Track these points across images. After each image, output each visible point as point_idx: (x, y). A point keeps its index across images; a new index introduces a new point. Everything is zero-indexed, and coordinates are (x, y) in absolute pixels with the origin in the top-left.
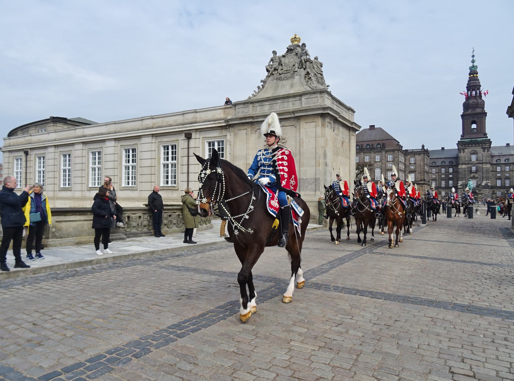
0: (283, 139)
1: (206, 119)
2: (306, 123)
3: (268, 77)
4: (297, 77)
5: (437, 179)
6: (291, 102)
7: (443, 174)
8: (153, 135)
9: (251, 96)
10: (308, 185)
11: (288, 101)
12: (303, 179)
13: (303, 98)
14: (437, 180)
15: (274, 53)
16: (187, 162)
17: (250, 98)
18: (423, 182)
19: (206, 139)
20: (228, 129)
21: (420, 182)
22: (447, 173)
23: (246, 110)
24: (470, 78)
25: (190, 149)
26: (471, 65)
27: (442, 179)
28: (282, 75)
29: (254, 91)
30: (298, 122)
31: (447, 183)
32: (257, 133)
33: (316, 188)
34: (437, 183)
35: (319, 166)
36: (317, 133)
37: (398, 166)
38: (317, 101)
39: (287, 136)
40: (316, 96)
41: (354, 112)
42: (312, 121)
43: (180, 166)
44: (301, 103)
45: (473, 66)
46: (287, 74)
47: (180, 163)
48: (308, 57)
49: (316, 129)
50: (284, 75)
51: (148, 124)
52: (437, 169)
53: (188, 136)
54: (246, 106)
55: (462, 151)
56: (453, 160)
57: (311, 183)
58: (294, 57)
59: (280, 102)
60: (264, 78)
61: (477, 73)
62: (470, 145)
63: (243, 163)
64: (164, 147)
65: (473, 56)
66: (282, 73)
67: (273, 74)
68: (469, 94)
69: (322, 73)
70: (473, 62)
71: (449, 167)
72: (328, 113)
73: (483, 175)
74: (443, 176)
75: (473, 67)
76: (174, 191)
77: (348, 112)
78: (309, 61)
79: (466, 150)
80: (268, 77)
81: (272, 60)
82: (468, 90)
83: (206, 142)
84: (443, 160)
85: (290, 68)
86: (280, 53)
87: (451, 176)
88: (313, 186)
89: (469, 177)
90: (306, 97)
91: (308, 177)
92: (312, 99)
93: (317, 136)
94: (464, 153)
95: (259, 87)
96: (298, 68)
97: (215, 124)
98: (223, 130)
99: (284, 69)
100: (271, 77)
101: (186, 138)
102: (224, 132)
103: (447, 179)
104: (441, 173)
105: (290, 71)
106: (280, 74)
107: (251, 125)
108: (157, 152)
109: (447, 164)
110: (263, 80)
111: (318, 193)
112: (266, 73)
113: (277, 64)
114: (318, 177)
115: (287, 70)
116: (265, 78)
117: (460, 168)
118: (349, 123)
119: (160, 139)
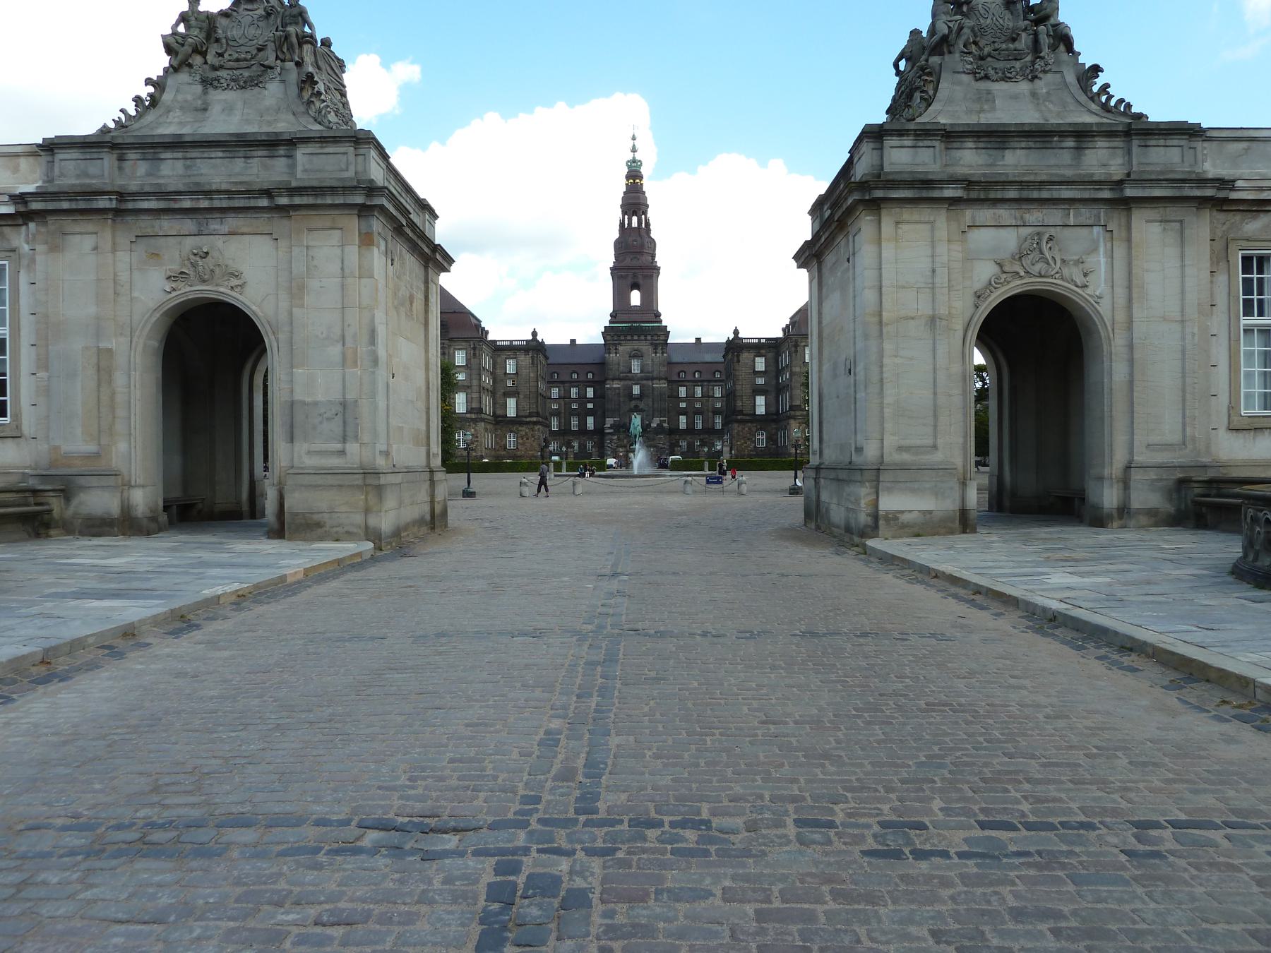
0: (232, 274)
2: (310, 230)
3: (171, 69)
6: (256, 160)
7: (575, 401)
9: (112, 125)
10: (321, 423)
12: (304, 403)
13: (301, 153)
14: (563, 415)
17: (105, 130)
18: (535, 419)
20: (24, 228)
21: (528, 419)
22: (582, 398)
26: (630, 156)
27: (573, 413)
29: (122, 111)
31: (583, 423)
33: (345, 431)
34: (563, 421)
35: (356, 366)
36: (346, 263)
37: (480, 379)
38: (344, 167)
40: (342, 150)
41: (436, 217)
44: (293, 167)
45: (634, 161)
46: (241, 71)
48: (307, 29)
49: (342, 251)
52: (562, 388)
54: (95, 156)
57: (328, 415)
58: (260, 24)
59: (220, 154)
60: (156, 72)
61: (641, 178)
62: (629, 337)
67: (190, 66)
69: (342, 88)
70: (634, 150)
72: (382, 208)
74: (575, 406)
77: (421, 214)
79: (621, 348)
80: (172, 70)
81: (183, 18)
82: (624, 213)
84: (573, 368)
85: (249, 56)
87: (590, 406)
88: (335, 427)
91: (320, 398)
92: (329, 156)
93: (347, 271)
94: (616, 353)
95: (138, 100)
99: (226, 56)
100: (183, 77)
106: (214, 68)
107: (113, 220)
110: (155, 79)
111: (352, 448)
112: (165, 60)
114: (350, 396)
115: (238, 60)
116: (161, 74)
118: (428, 247)
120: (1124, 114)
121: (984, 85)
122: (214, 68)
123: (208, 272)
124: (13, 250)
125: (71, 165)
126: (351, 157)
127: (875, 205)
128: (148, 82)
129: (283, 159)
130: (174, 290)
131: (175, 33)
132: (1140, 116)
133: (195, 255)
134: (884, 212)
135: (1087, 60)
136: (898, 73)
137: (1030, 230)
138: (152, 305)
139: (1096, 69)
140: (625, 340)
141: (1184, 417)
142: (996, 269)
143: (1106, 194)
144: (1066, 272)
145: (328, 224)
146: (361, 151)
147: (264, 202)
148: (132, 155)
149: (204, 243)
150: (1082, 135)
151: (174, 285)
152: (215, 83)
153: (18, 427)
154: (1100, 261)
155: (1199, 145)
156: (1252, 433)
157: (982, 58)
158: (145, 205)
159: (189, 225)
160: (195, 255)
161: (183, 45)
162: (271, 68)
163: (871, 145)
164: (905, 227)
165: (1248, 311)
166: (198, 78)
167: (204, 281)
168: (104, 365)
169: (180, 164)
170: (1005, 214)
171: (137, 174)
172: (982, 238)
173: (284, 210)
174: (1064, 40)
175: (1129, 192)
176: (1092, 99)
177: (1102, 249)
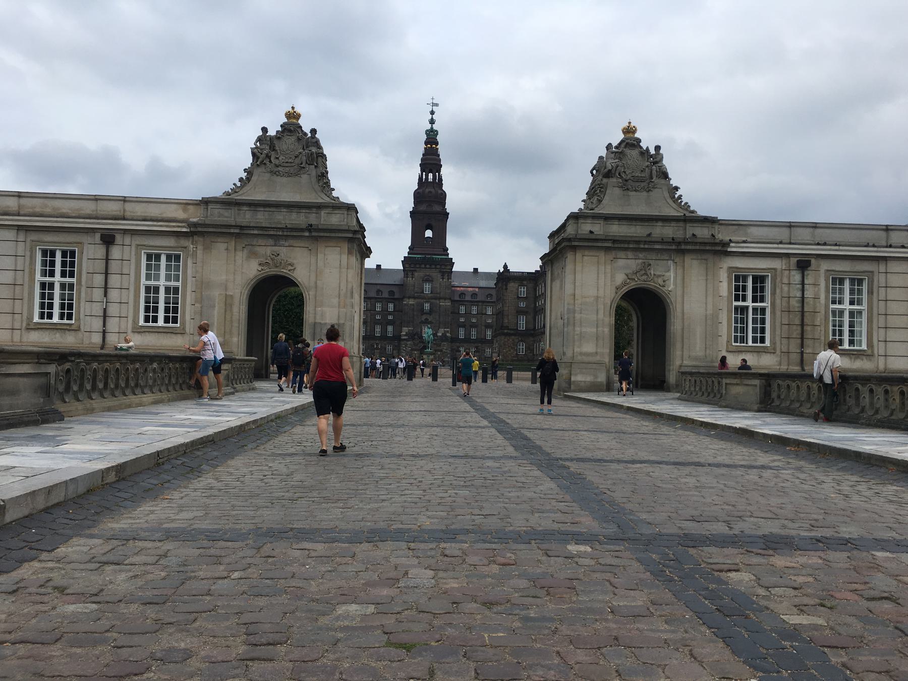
1: (146, 215)
2: (326, 246)
4: (305, 177)
5: (369, 320)
7: (379, 313)
8: (19, 228)
11: (299, 211)
13: (323, 213)
14: (369, 324)
15: (264, 130)
16: (104, 283)
19: (144, 247)
22: (385, 311)
23: (226, 213)
24: (425, 148)
25: (110, 261)
26: (429, 127)
27: (377, 322)
28: (280, 169)
29: (234, 184)
30: (313, 243)
31: (384, 330)
32: (245, 249)
34: (368, 328)
39: (295, 262)
42: (335, 245)
43: (83, 289)
45: (432, 130)
47: (83, 283)
50: (283, 168)
51: (8, 207)
52: (369, 303)
53: (108, 239)
55: (410, 274)
56: (395, 289)
61: (437, 144)
62: (423, 266)
63: (220, 294)
64: (44, 253)
65: (432, 113)
67: (265, 164)
68: (424, 177)
70: (432, 122)
71: (389, 300)
73: (439, 318)
74: (378, 317)
75: (432, 132)
76: (67, 332)
78: (321, 156)
79: (416, 274)
81: (259, 139)
82: (422, 171)
83: (143, 253)
84: (378, 287)
86: (272, 132)
87: (390, 317)
89: (420, 321)
90: (327, 212)
91: (328, 321)
94: (412, 278)
96: (307, 163)
97: (167, 226)
98: (180, 237)
100: (260, 170)
101: (101, 242)
102: (184, 242)
103: (385, 323)
104: (375, 310)
106: (277, 166)
108: (28, 259)
109: (386, 295)
113: (268, 147)
117: (405, 304)
119: (34, 236)
120: (686, 210)
121: (625, 193)
122: (277, 166)
123: (278, 262)
124: (186, 248)
125: (216, 211)
126: (346, 216)
127: (574, 248)
128: (245, 170)
130: (262, 270)
131: (257, 147)
132: (693, 212)
133: (273, 255)
135: (674, 183)
136: (593, 175)
137: (641, 261)
138: (252, 276)
139: (677, 188)
140: (420, 268)
141: (706, 345)
142: (626, 277)
143: (674, 247)
144: (656, 279)
145: (335, 245)
146: (350, 213)
147: (307, 234)
148: (245, 208)
150: (666, 220)
151: (262, 268)
153: (184, 329)
155: (717, 226)
156: (737, 354)
157: (626, 181)
158: (252, 232)
159: (271, 242)
160: (273, 255)
161: (261, 154)
162: (304, 168)
163: (574, 221)
164: (586, 258)
167: (277, 267)
168: (228, 302)
169: (266, 213)
171: (246, 217)
172: (621, 263)
173: (316, 239)
175: (683, 247)
176: (674, 202)
177: (672, 271)
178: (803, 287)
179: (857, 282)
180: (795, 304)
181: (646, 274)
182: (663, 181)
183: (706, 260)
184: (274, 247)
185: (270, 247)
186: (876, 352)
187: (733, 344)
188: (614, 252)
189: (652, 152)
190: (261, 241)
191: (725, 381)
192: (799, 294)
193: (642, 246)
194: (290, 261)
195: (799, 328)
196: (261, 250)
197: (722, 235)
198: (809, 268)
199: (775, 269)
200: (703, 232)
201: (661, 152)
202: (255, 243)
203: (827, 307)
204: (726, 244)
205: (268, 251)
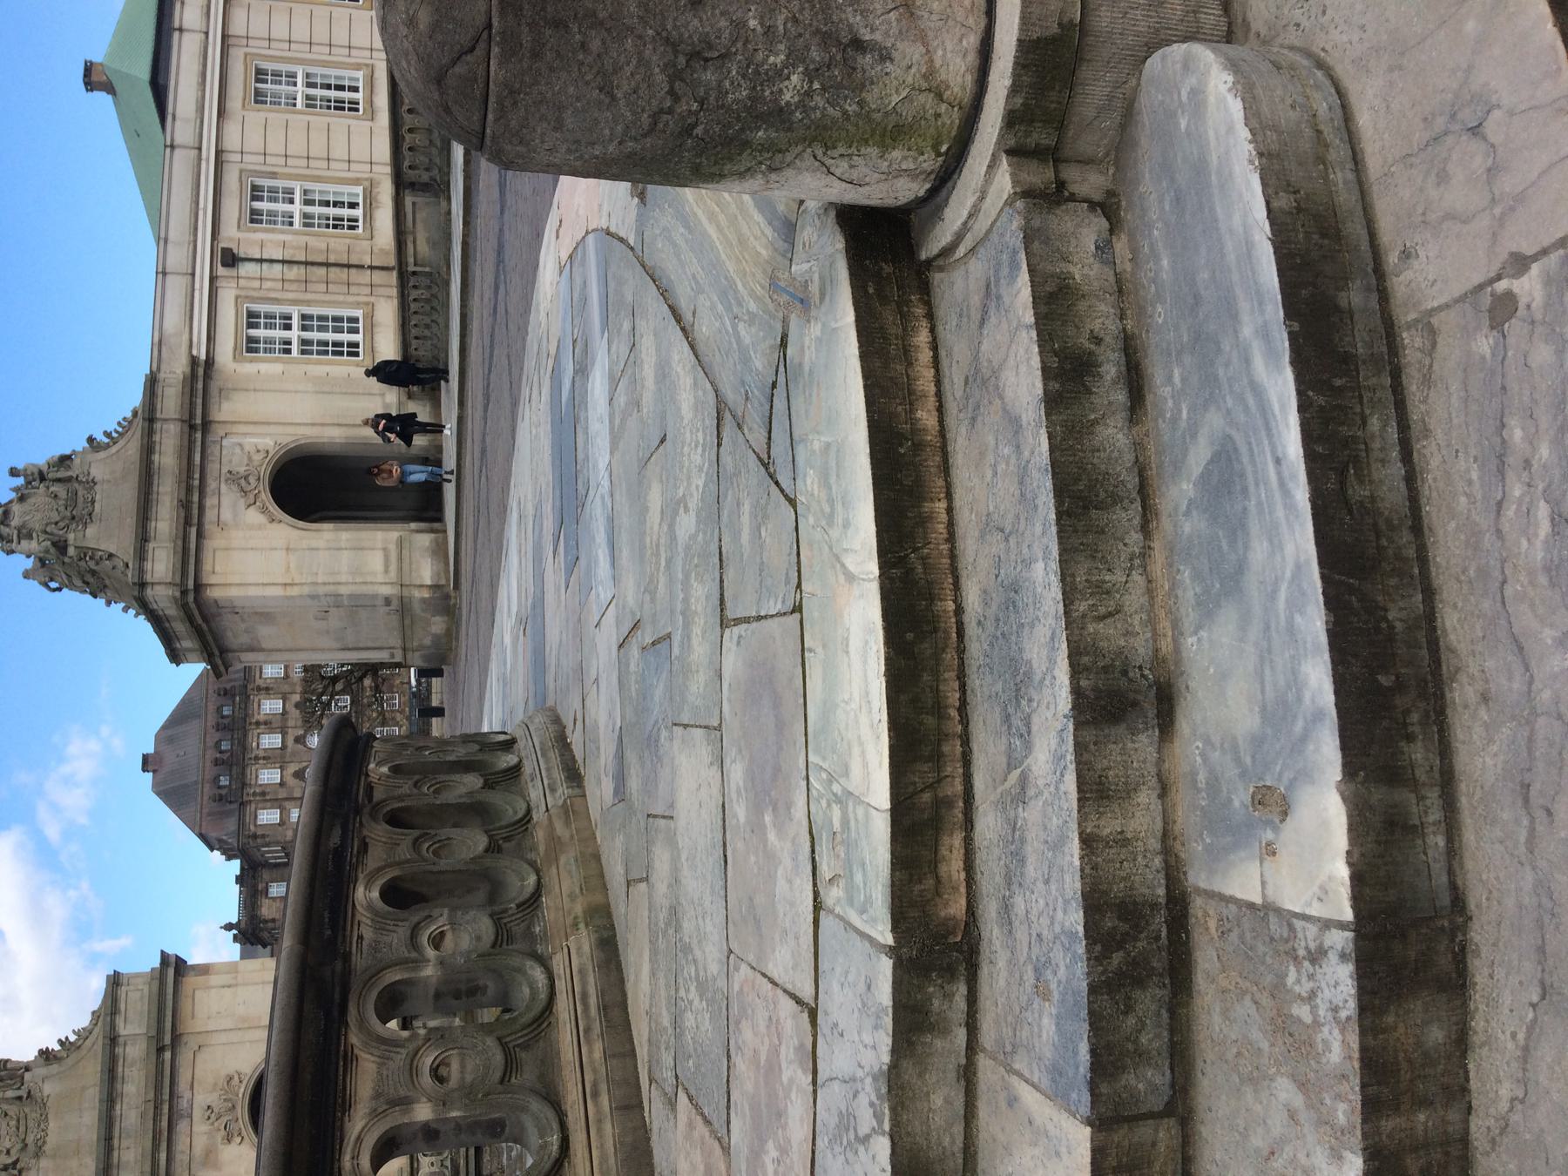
2: (193, 1017)
4: (48, 1089)
11: (120, 1080)
40: (123, 996)
42: (190, 1000)
66: (24, 1140)
105: (22, 1115)
127: (199, 587)
129: (127, 1049)
132: (135, 413)
134: (205, 582)
135: (81, 444)
136: (59, 589)
139: (91, 440)
142: (252, 508)
143: (199, 435)
144: (256, 463)
145: (190, 1000)
147: (168, 1055)
149: (198, 1113)
150: (148, 450)
152: (39, 1143)
154: (249, 442)
155: (162, 376)
159: (182, 1126)
164: (217, 568)
165: (288, 351)
166: (33, 1161)
169: (124, 1144)
170: (210, 502)
172: (226, 515)
173: (176, 1038)
174: (64, 460)
175: (199, 421)
178: (266, 260)
179: (256, 193)
180: (294, 272)
181: (246, 478)
182: (77, 461)
183: (220, 391)
184: (195, 1119)
185: (195, 1129)
186: (366, 176)
187: (361, 358)
188: (207, 527)
189: (20, 481)
190: (181, 1143)
191: (411, 268)
192: (278, 267)
193: (196, 483)
194: (222, 1082)
195: (332, 269)
196: (200, 1143)
197: (177, 368)
198: (235, 251)
199: (237, 298)
200: (171, 403)
201: (20, 466)
202: (186, 1158)
203: (296, 233)
204: (194, 361)
205: (201, 1128)
